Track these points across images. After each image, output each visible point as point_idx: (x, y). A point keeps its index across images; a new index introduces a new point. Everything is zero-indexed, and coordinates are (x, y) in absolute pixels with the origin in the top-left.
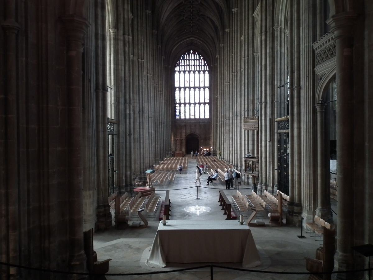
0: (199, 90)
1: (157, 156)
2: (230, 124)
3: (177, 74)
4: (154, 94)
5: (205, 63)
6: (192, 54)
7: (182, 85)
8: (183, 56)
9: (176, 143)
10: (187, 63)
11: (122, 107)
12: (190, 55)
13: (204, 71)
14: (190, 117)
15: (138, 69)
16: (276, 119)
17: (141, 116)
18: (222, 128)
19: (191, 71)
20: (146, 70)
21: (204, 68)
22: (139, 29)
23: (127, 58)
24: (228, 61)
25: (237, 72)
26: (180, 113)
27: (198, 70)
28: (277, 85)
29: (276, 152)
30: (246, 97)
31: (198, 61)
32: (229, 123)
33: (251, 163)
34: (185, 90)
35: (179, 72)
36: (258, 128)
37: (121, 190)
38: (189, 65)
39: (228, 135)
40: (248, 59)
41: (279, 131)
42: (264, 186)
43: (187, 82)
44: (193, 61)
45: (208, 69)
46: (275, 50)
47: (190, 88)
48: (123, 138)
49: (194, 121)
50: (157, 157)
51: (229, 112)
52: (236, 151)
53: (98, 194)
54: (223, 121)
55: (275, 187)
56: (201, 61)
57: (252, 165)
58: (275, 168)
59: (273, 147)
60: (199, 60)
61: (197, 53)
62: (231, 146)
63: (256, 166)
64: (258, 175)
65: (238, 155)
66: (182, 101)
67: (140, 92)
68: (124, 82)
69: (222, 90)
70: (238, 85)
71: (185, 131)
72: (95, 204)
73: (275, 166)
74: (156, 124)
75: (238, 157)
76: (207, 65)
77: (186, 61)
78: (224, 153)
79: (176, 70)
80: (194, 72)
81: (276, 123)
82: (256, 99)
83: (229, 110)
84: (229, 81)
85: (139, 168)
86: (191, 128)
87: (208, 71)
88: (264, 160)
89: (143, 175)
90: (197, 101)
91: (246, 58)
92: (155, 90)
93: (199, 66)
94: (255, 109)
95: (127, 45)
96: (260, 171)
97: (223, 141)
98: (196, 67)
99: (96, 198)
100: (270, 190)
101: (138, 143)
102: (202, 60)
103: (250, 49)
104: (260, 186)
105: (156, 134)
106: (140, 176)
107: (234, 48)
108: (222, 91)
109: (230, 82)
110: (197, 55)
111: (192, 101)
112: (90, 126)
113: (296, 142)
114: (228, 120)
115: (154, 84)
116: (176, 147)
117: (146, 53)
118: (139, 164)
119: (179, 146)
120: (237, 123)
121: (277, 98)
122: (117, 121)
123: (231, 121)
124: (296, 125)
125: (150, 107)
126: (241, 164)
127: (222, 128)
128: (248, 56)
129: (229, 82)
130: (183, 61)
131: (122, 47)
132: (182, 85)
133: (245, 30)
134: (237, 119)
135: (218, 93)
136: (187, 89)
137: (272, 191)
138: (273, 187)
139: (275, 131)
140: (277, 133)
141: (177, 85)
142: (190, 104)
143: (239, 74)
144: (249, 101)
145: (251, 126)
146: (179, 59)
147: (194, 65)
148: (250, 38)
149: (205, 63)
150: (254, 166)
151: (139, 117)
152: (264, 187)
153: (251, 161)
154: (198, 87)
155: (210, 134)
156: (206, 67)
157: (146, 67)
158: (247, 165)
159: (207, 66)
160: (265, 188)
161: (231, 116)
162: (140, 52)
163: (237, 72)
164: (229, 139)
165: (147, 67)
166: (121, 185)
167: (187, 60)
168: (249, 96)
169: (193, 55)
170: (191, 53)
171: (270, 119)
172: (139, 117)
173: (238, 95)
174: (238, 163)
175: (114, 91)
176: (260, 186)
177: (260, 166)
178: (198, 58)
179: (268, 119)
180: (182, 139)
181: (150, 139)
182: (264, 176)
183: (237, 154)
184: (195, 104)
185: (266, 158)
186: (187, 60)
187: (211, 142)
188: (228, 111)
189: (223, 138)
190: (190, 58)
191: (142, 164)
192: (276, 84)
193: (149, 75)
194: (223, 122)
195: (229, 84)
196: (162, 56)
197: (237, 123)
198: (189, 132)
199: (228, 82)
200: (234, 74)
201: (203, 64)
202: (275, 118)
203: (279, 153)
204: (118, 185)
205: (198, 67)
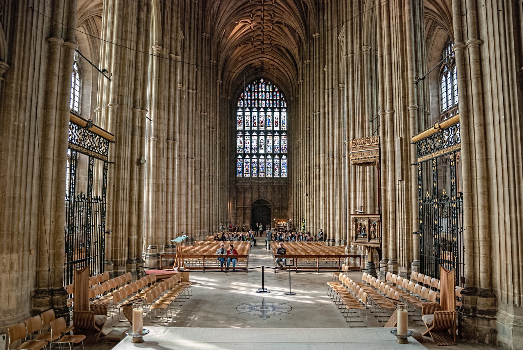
0: (273, 136)
1: (202, 226)
2: (321, 176)
3: (240, 113)
4: (201, 128)
5: (282, 96)
6: (262, 84)
7: (247, 128)
8: (249, 86)
9: (236, 214)
10: (255, 96)
11: (127, 113)
12: (260, 85)
13: (280, 109)
14: (258, 175)
15: (170, 69)
16: (413, 139)
17: (171, 146)
18: (308, 185)
19: (261, 108)
20: (187, 83)
21: (280, 104)
22: (175, 8)
23: (142, 29)
24: (318, 79)
25: (332, 88)
26: (243, 168)
27: (271, 106)
28: (412, 78)
29: (414, 200)
30: (351, 118)
31: (271, 94)
32: (319, 175)
33: (366, 223)
34: (251, 135)
35: (244, 109)
36: (380, 157)
37: (117, 269)
38: (258, 100)
39: (318, 193)
40: (352, 57)
41: (420, 160)
42: (392, 266)
43: (255, 123)
44: (264, 94)
45: (285, 106)
46: (405, 19)
47: (258, 132)
48: (126, 171)
49: (264, 181)
50: (202, 228)
51: (319, 157)
52: (331, 216)
53: (39, 264)
54: (309, 174)
55: (413, 267)
56: (275, 94)
57: (367, 227)
58: (412, 230)
59: (408, 191)
60: (273, 92)
61: (269, 83)
62: (322, 211)
63: (375, 229)
64: (379, 246)
65: (336, 222)
66: (247, 151)
67: (171, 107)
68: (134, 70)
69: (308, 127)
70: (334, 108)
71: (250, 196)
72: (29, 286)
73: (412, 226)
74: (202, 175)
75: (336, 227)
76: (284, 99)
77: (253, 93)
78: (310, 225)
79: (239, 106)
80: (266, 109)
81: (412, 146)
82: (368, 120)
83: (319, 154)
84: (319, 109)
85: (164, 237)
86: (259, 192)
87: (285, 108)
88: (390, 216)
89: (170, 249)
90: (269, 150)
91: (350, 56)
92: (202, 121)
93: (273, 100)
94: (367, 136)
95: (145, 8)
96: (383, 237)
97: (309, 205)
98: (268, 102)
99: (31, 272)
100: (402, 273)
101: (164, 194)
102: (277, 92)
103: (356, 41)
104: (384, 265)
105: (202, 190)
106: (165, 251)
107: (328, 52)
108: (308, 129)
109: (321, 110)
110: (269, 85)
111: (262, 152)
112: (23, 105)
113: (478, 155)
114: (318, 171)
115: (201, 112)
116: (237, 219)
117: (187, 56)
118: (164, 230)
119: (242, 218)
120: (333, 169)
121: (413, 101)
122: (116, 138)
123: (322, 171)
124: (476, 119)
125: (190, 141)
126: (340, 238)
127: (308, 185)
128: (353, 53)
129: (319, 111)
130: (249, 93)
131: (134, 10)
132: (247, 128)
133: (346, 14)
134: (333, 164)
135: (301, 135)
136: (255, 134)
137: (407, 274)
138: (409, 267)
139: (410, 161)
140: (416, 165)
141: (240, 128)
142: (258, 155)
143: (336, 92)
144: (357, 124)
145: (365, 154)
146: (243, 91)
147: (266, 100)
148: (355, 25)
149: (282, 96)
150: (372, 229)
151: (168, 149)
152: (390, 267)
153: (367, 221)
154: (270, 131)
155: (288, 200)
156: (282, 102)
157: (187, 78)
158: (359, 227)
159: (284, 101)
160: (394, 269)
161: (322, 163)
162: (173, 42)
163: (332, 88)
164: (319, 201)
165: (189, 79)
166: (118, 259)
167: (255, 92)
168: (356, 117)
169: (264, 85)
170: (260, 82)
171: (401, 139)
172: (168, 149)
173: (335, 125)
174: (336, 235)
175: (115, 84)
176: (384, 265)
177: (383, 228)
178: (271, 90)
179: (397, 140)
180: (246, 208)
181: (190, 193)
182: (391, 247)
183: (333, 220)
184: (265, 155)
185: (394, 212)
186: (255, 92)
187: (290, 213)
188: (318, 156)
189: (309, 202)
190: (260, 90)
191: (169, 231)
192: (409, 76)
193: (191, 91)
194: (309, 176)
195: (319, 114)
196: (217, 79)
197: (333, 169)
198: (256, 197)
199: (317, 110)
200: (328, 92)
201: (278, 98)
202: (411, 136)
203: (421, 201)
204: (113, 260)
205: (271, 102)
